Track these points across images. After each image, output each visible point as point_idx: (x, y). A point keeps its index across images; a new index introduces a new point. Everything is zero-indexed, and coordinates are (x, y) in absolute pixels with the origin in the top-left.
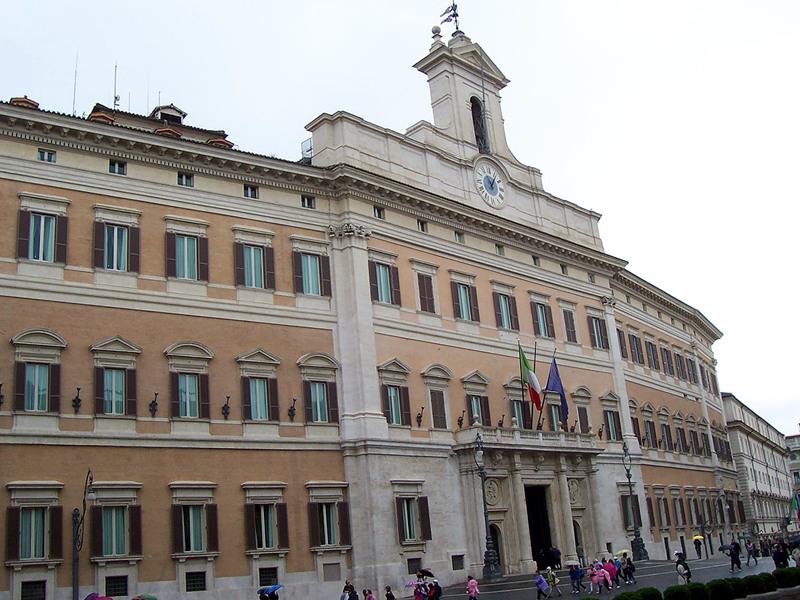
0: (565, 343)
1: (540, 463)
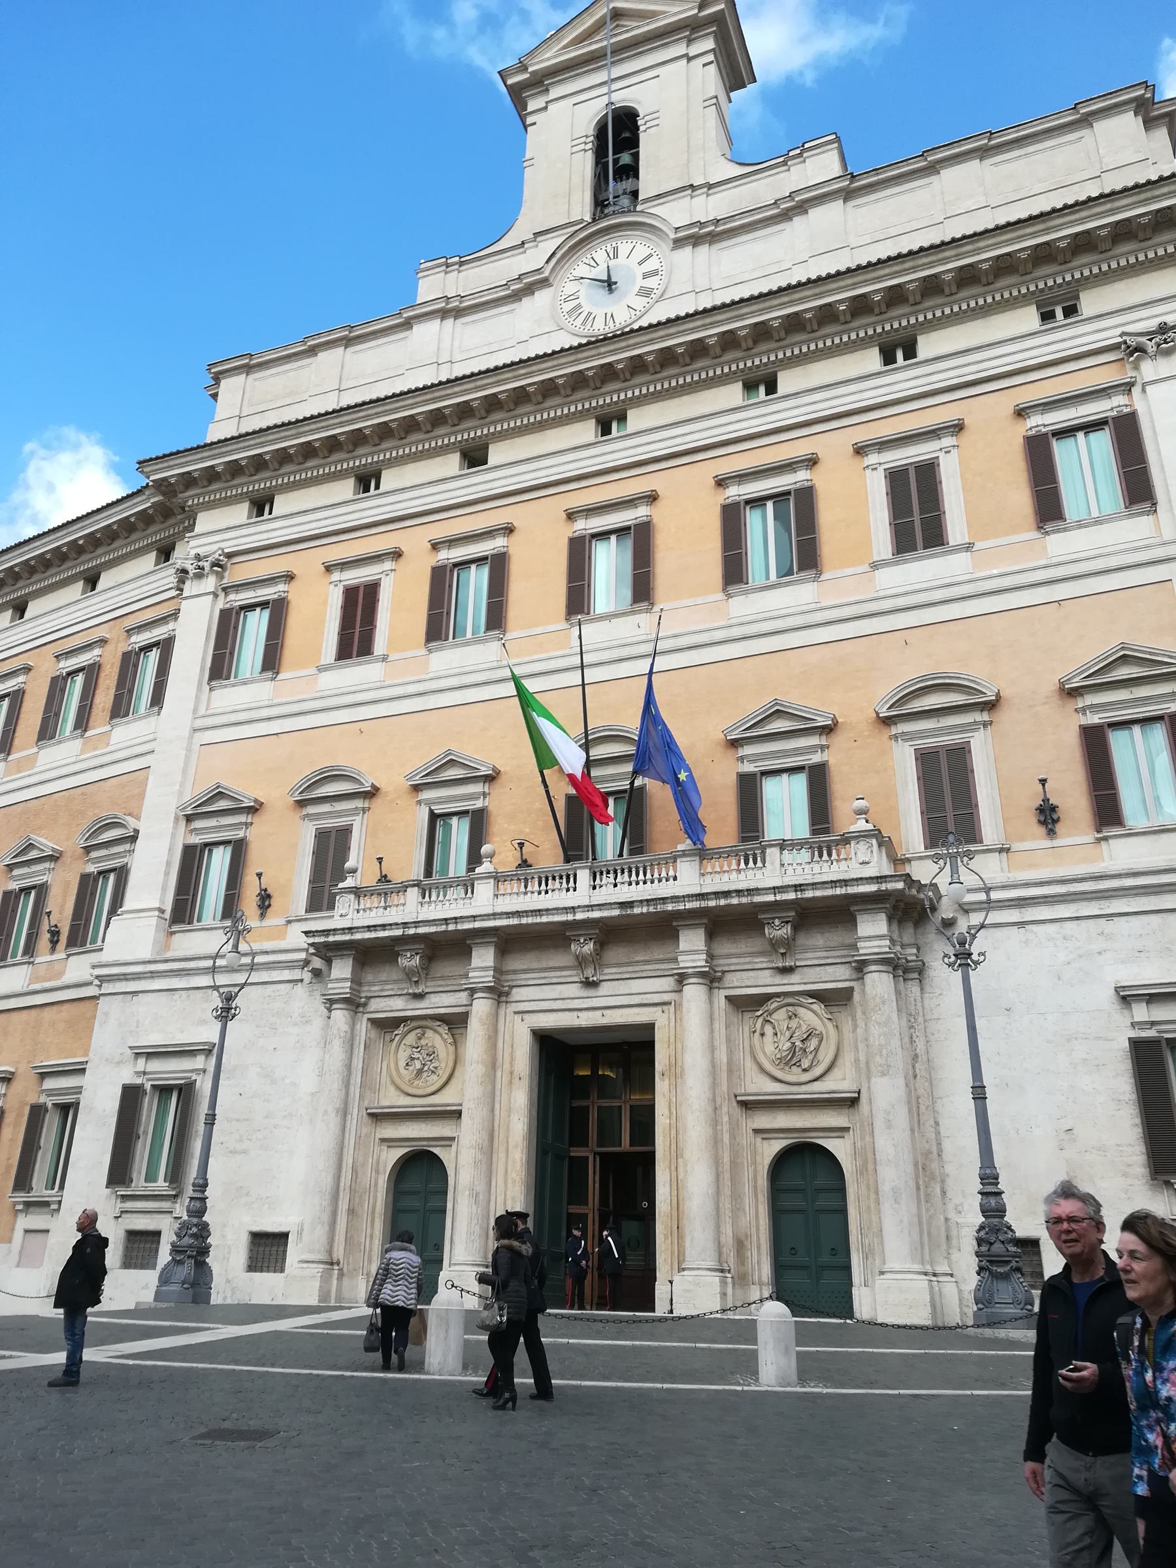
1: (596, 960)
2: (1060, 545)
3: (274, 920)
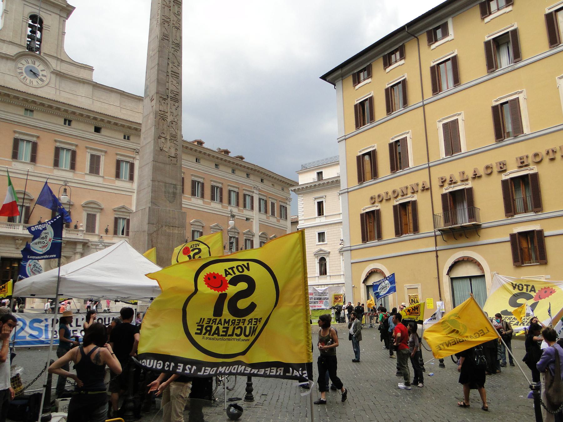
0: (86, 174)
2: (119, 183)
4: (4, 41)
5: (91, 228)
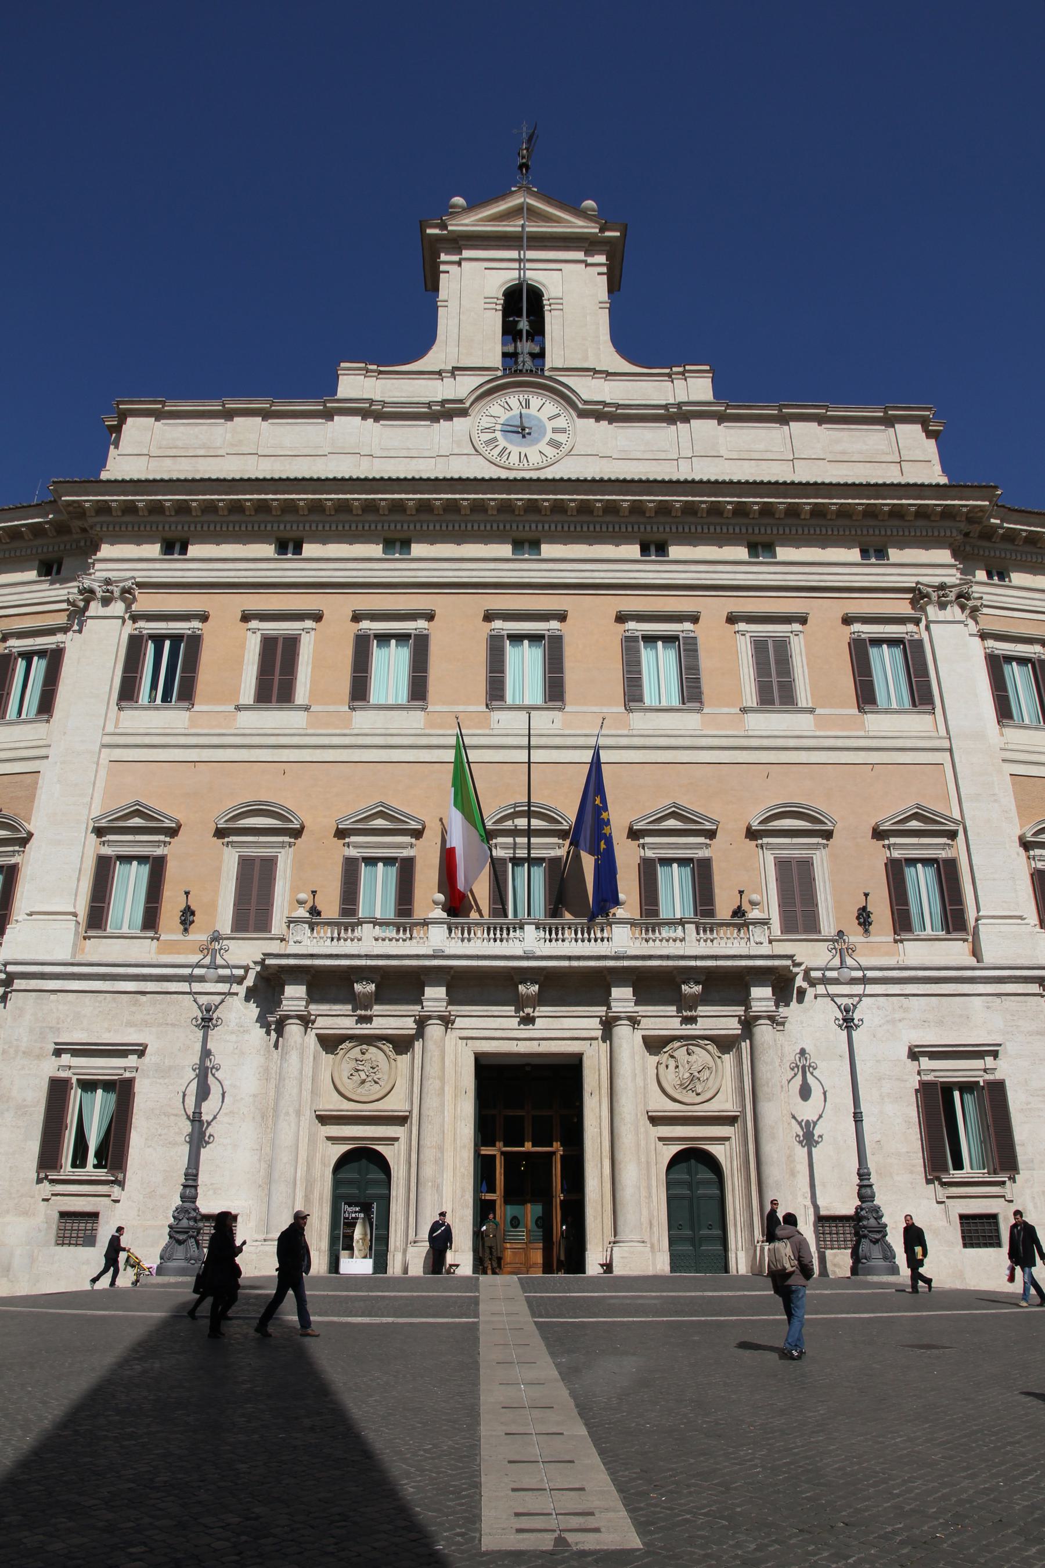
0: (744, 710)
2: (875, 723)
3: (199, 935)
4: (439, 373)
5: (800, 913)
